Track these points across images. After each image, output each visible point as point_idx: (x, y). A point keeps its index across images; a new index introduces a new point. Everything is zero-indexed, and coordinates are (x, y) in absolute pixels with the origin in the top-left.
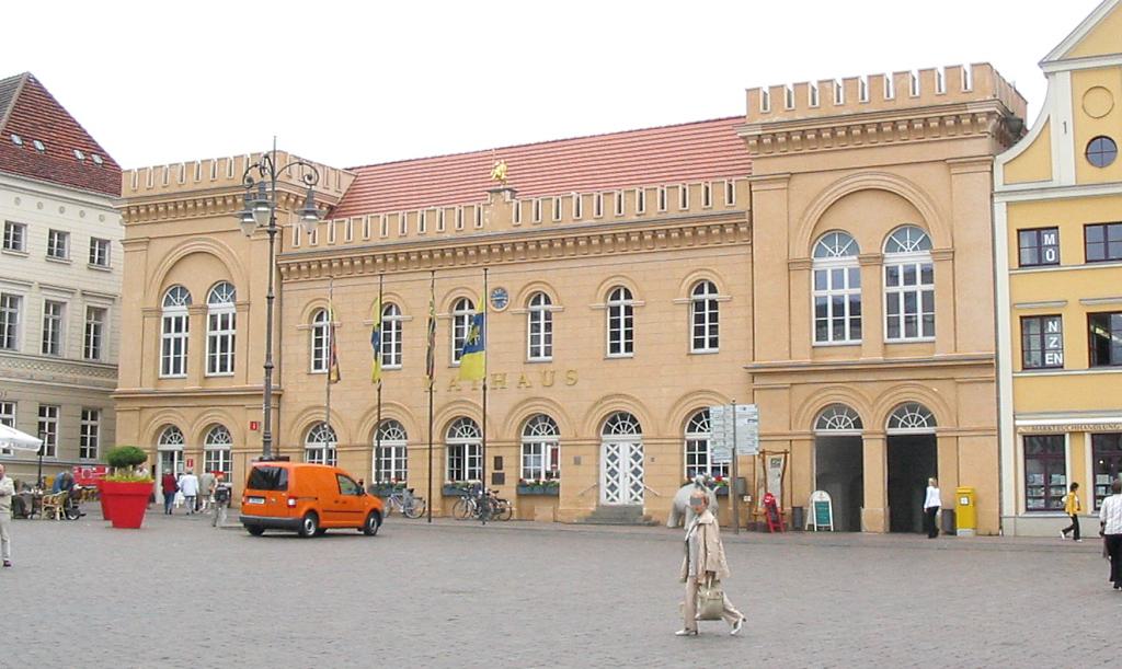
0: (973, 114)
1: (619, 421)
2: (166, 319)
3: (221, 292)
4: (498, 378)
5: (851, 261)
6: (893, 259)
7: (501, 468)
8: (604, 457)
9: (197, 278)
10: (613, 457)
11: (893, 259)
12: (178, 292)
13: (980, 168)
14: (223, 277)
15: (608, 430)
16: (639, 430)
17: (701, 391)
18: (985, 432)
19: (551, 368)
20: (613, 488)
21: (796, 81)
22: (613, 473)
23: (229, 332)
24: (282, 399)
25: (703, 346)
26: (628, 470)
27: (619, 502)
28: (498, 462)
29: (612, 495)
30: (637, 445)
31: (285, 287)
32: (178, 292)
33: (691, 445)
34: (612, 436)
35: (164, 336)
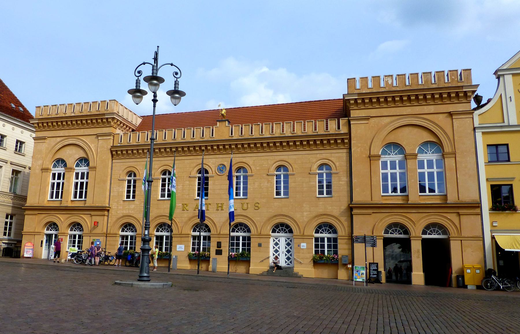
0: (465, 92)
1: (282, 227)
4: (220, 205)
5: (399, 157)
6: (420, 157)
7: (220, 247)
8: (272, 244)
9: (71, 155)
10: (276, 244)
11: (420, 157)
12: (60, 162)
13: (468, 116)
14: (82, 155)
15: (274, 231)
16: (291, 231)
17: (286, 216)
18: (474, 238)
19: (247, 201)
21: (374, 75)
22: (276, 251)
23: (85, 181)
24: (110, 211)
26: (285, 250)
28: (219, 244)
30: (288, 239)
32: (60, 162)
33: (317, 239)
34: (276, 234)
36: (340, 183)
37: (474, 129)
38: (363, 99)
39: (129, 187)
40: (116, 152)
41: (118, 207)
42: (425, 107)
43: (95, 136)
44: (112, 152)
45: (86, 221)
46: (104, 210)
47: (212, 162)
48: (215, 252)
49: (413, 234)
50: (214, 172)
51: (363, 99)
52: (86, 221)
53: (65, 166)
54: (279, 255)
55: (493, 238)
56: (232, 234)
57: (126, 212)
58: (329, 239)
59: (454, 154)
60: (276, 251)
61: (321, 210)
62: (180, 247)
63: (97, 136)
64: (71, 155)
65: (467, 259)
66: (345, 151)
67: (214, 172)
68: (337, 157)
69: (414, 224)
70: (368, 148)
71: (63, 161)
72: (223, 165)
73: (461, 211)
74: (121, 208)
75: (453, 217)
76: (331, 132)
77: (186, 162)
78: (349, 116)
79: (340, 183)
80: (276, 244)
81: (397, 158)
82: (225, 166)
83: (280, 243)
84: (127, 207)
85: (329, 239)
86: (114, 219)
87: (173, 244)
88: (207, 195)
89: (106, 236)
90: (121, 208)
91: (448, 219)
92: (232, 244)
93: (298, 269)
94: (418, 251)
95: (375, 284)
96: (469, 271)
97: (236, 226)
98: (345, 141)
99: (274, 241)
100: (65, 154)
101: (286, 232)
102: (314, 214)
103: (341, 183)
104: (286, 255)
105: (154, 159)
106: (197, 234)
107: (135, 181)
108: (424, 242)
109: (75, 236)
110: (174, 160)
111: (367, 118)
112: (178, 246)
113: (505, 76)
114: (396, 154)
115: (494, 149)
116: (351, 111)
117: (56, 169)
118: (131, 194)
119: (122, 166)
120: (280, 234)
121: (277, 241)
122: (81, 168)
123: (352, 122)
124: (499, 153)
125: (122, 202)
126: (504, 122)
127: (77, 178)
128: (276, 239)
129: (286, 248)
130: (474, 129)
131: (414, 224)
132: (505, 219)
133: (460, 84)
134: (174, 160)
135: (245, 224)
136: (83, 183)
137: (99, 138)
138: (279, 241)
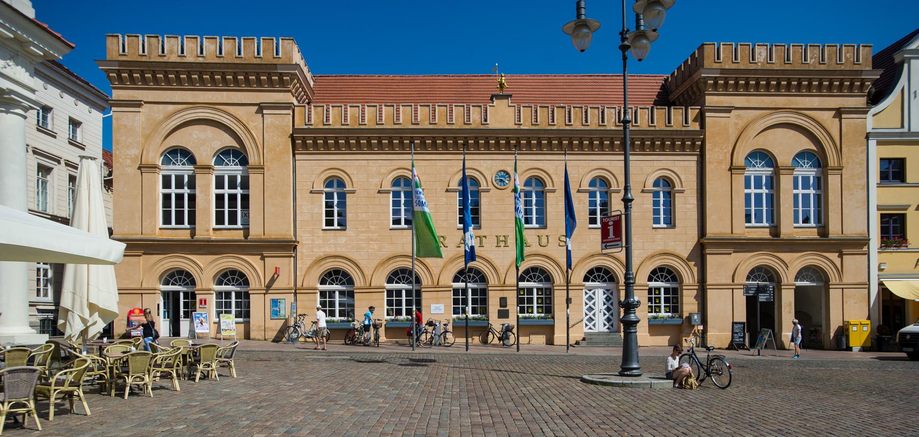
4: (502, 238)
5: (769, 171)
7: (506, 306)
9: (205, 143)
14: (229, 141)
15: (586, 279)
27: (595, 330)
28: (503, 302)
29: (591, 325)
30: (608, 290)
31: (297, 157)
36: (686, 206)
38: (726, 80)
39: (329, 205)
40: (304, 141)
41: (313, 240)
42: (808, 99)
43: (256, 108)
44: (293, 139)
45: (254, 267)
46: (288, 247)
47: (485, 166)
48: (497, 314)
49: (784, 281)
50: (490, 183)
51: (726, 80)
52: (254, 267)
54: (594, 315)
55: (881, 284)
56: (521, 284)
57: (331, 250)
58: (667, 290)
59: (840, 169)
60: (590, 309)
61: (660, 248)
62: (436, 308)
63: (261, 108)
64: (205, 143)
65: (851, 311)
66: (695, 158)
67: (490, 183)
68: (682, 168)
70: (729, 156)
72: (504, 172)
74: (321, 242)
75: (834, 256)
76: (675, 128)
77: (439, 163)
78: (703, 104)
79: (686, 206)
81: (765, 172)
82: (507, 173)
83: (596, 298)
84: (332, 241)
85: (667, 290)
86: (309, 262)
87: (424, 303)
88: (476, 221)
89: (295, 294)
90: (321, 242)
91: (825, 261)
92: (456, 302)
94: (790, 305)
95: (741, 351)
96: (855, 328)
97: (527, 272)
98: (694, 144)
99: (586, 293)
100: (190, 138)
101: (605, 281)
102: (650, 252)
103: (687, 206)
104: (605, 314)
105: (631, 158)
106: (461, 285)
108: (799, 291)
110: (464, 160)
111: (728, 110)
112: (433, 306)
113: (912, 61)
114: (763, 166)
115: (886, 163)
116: (707, 97)
117: (171, 167)
118: (336, 218)
119: (315, 168)
120: (596, 284)
122: (177, 167)
123: (707, 114)
124: (894, 171)
125: (321, 232)
127: (748, 186)
131: (787, 267)
132: (898, 260)
133: (856, 68)
134: (464, 160)
135: (756, 267)
137: (265, 112)
138: (594, 293)
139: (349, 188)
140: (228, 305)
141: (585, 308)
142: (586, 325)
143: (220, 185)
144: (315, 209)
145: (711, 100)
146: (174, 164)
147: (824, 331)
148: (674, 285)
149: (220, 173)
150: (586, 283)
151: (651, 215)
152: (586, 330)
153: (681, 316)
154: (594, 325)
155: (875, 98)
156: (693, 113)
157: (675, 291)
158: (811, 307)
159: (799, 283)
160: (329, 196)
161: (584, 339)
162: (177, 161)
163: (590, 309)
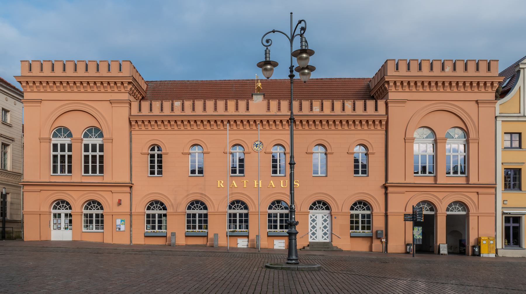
1: (321, 204)
2: (85, 145)
3: (91, 133)
9: (77, 124)
14: (93, 123)
15: (311, 208)
20: (314, 234)
25: (236, 173)
27: (317, 240)
29: (314, 237)
34: (314, 211)
35: (84, 153)
37: (496, 117)
49: (439, 211)
52: (108, 199)
53: (70, 135)
54: (316, 231)
60: (314, 227)
63: (111, 102)
64: (77, 124)
68: (375, 138)
69: (441, 202)
71: (66, 130)
73: (480, 190)
75: (474, 196)
80: (314, 221)
85: (363, 216)
93: (336, 243)
99: (311, 217)
101: (323, 209)
104: (323, 230)
107: (160, 156)
109: (91, 216)
111: (403, 101)
117: (58, 139)
119: (144, 139)
120: (318, 211)
121: (314, 217)
123: (389, 105)
126: (520, 113)
128: (314, 215)
129: (323, 224)
130: (496, 117)
136: (88, 156)
137: (113, 105)
138: (316, 217)
139: (164, 151)
140: (91, 222)
141: (310, 227)
142: (311, 237)
143: (86, 150)
144: (142, 164)
145: (392, 96)
146: (60, 137)
147: (466, 244)
148: (368, 212)
149: (87, 143)
150: (311, 211)
151: (353, 169)
152: (310, 240)
153: (372, 232)
154: (316, 237)
155: (502, 93)
156: (381, 103)
157: (369, 216)
158: (457, 226)
159: (449, 213)
160: (152, 156)
161: (308, 246)
162: (61, 135)
163: (314, 227)
